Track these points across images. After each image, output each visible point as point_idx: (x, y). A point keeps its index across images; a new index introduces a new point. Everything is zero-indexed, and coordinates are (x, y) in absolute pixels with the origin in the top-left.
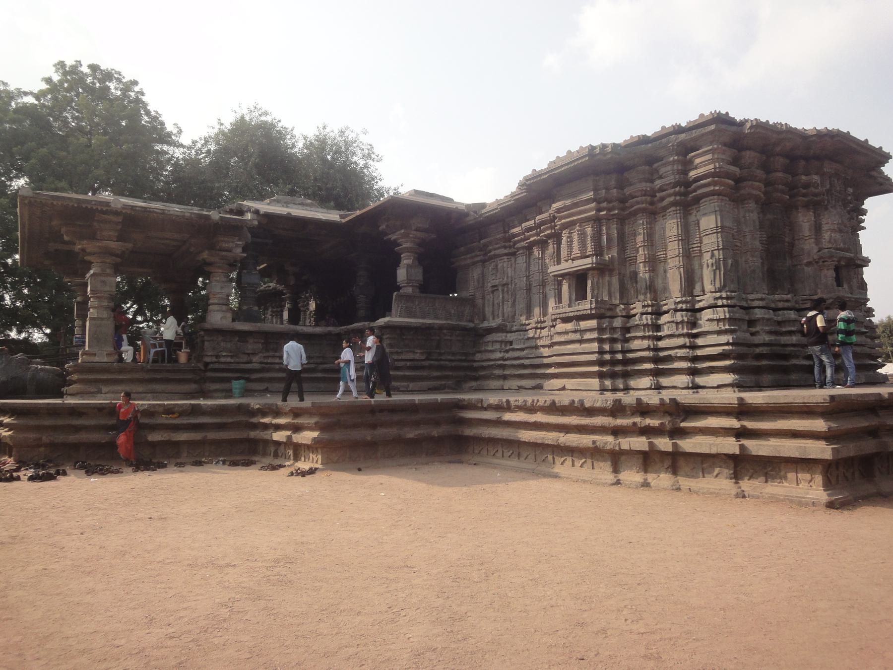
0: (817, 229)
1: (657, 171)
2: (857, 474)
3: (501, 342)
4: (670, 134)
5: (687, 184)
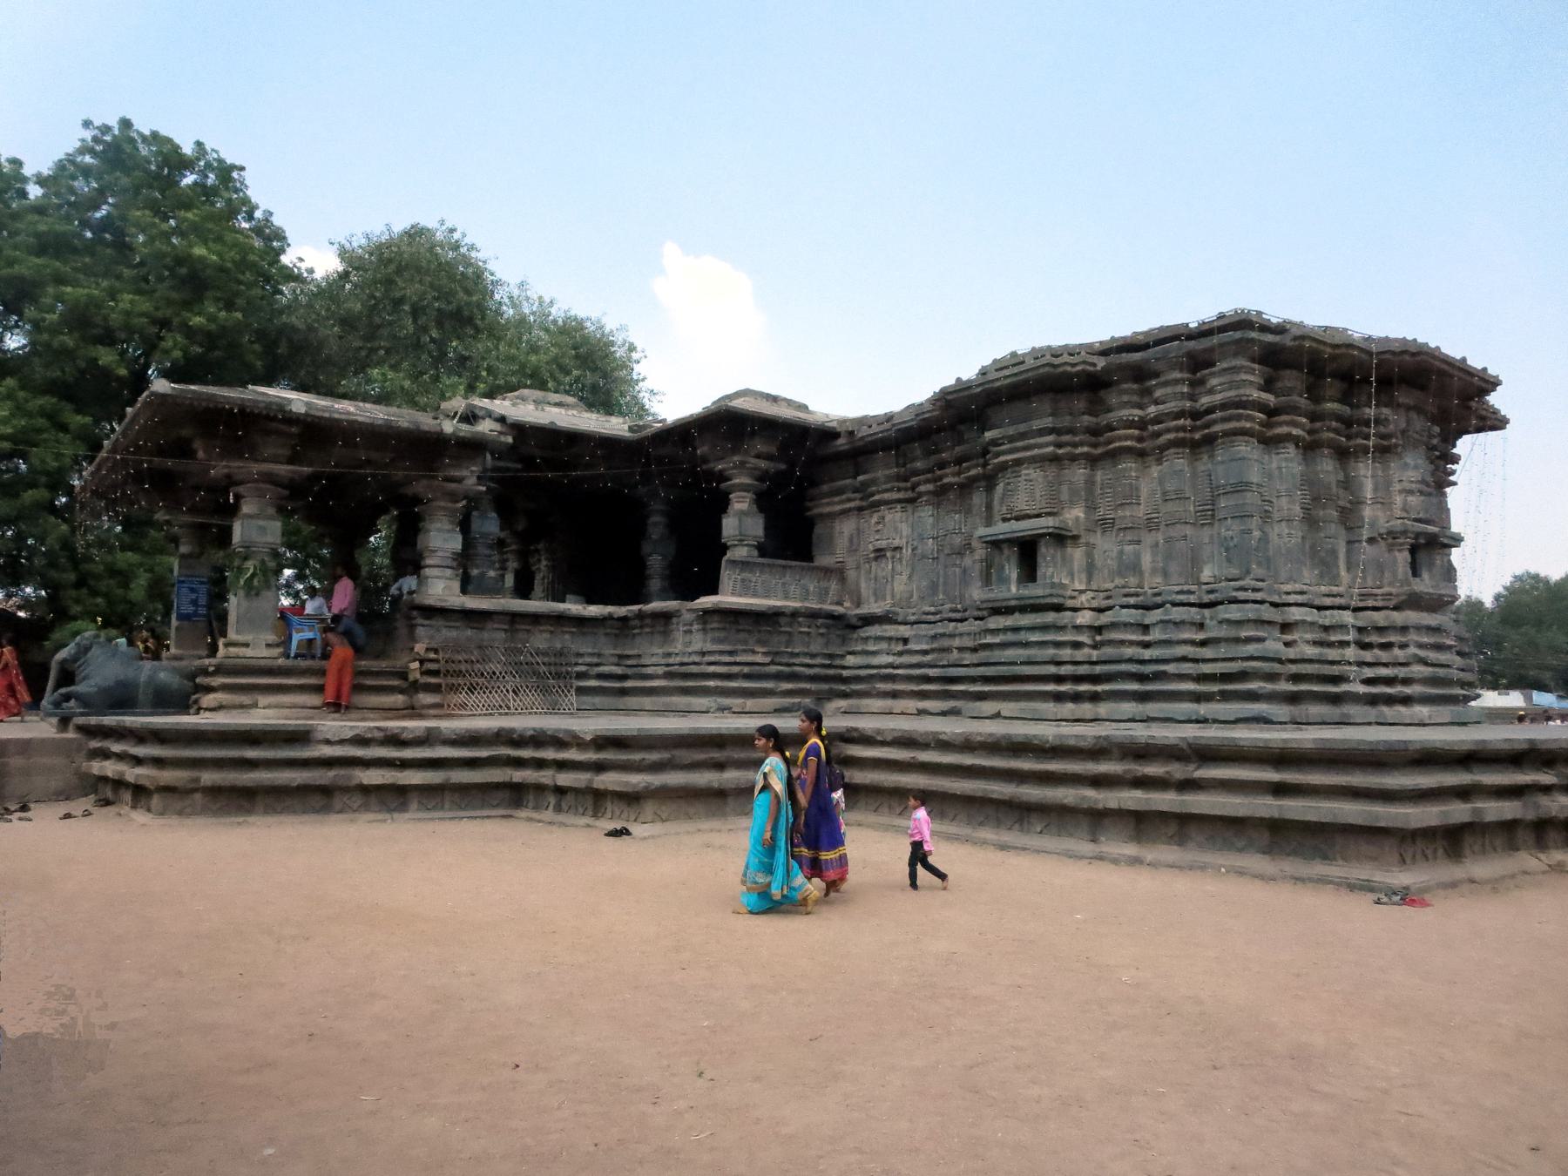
0: (1383, 487)
1: (1148, 392)
2: (1440, 851)
3: (890, 639)
4: (1176, 338)
5: (1195, 415)
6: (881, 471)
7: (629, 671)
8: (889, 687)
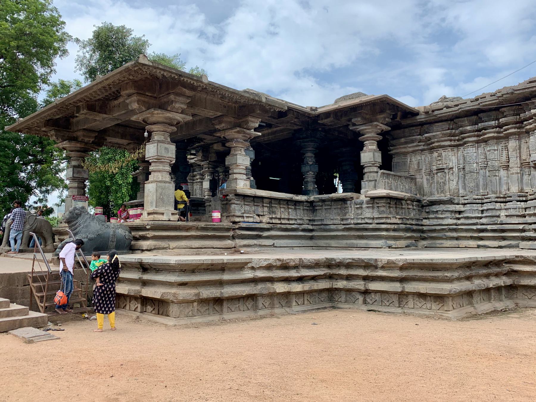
3: (452, 212)
6: (437, 133)
7: (314, 227)
8: (455, 234)
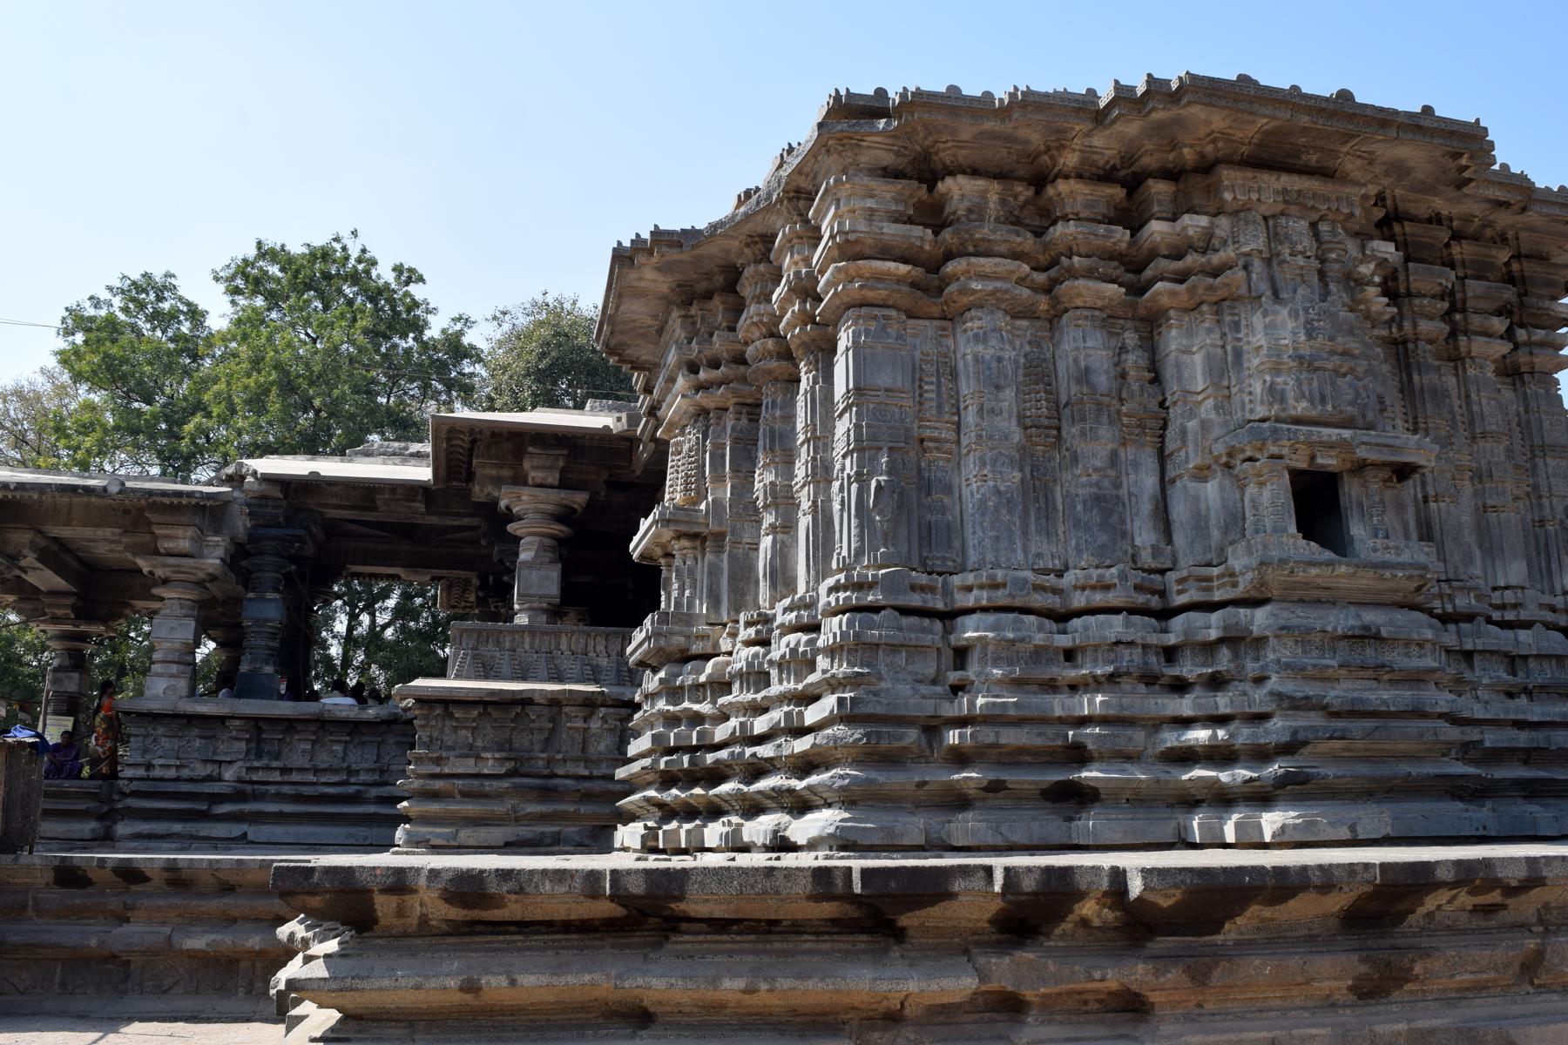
0: (1225, 367)
